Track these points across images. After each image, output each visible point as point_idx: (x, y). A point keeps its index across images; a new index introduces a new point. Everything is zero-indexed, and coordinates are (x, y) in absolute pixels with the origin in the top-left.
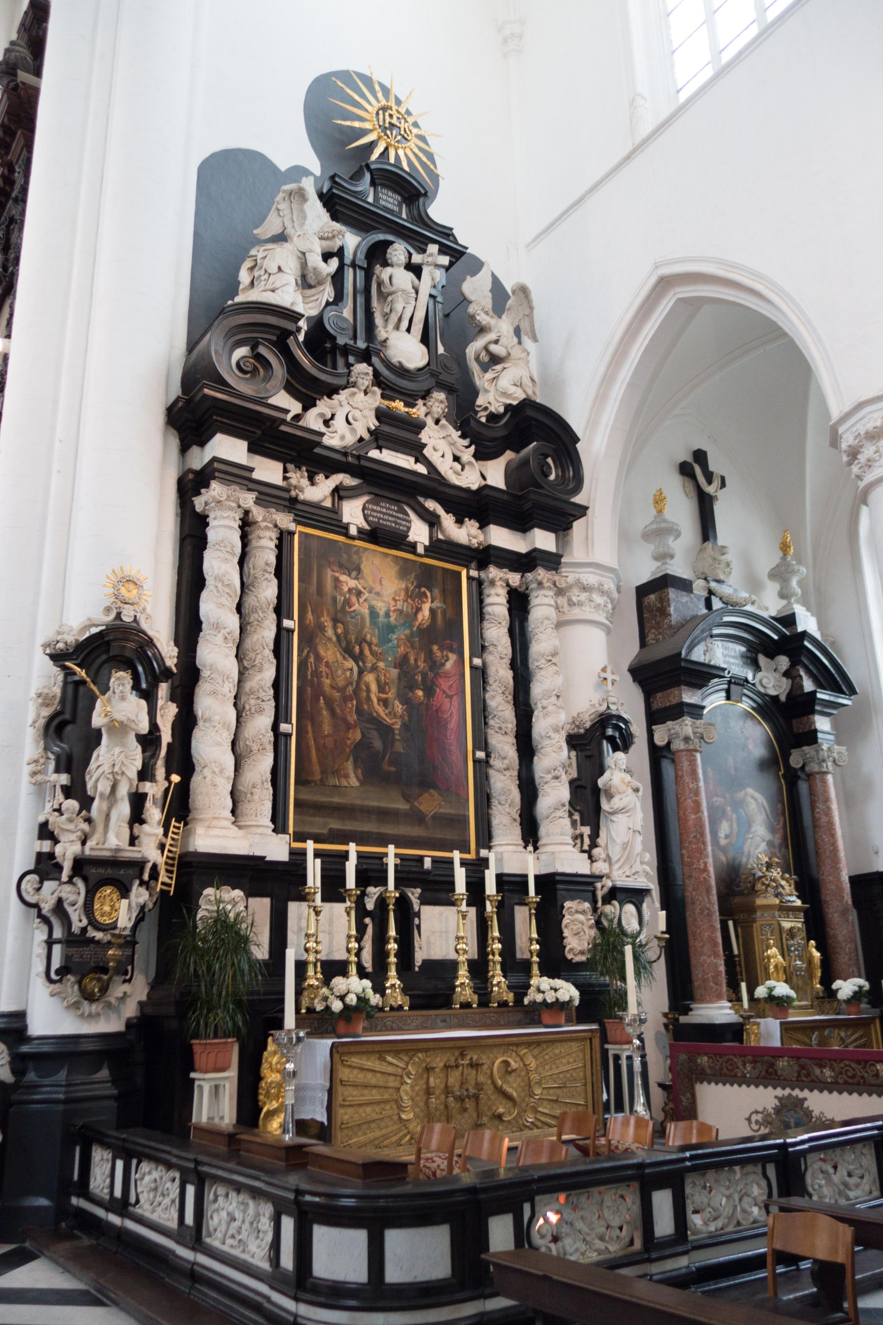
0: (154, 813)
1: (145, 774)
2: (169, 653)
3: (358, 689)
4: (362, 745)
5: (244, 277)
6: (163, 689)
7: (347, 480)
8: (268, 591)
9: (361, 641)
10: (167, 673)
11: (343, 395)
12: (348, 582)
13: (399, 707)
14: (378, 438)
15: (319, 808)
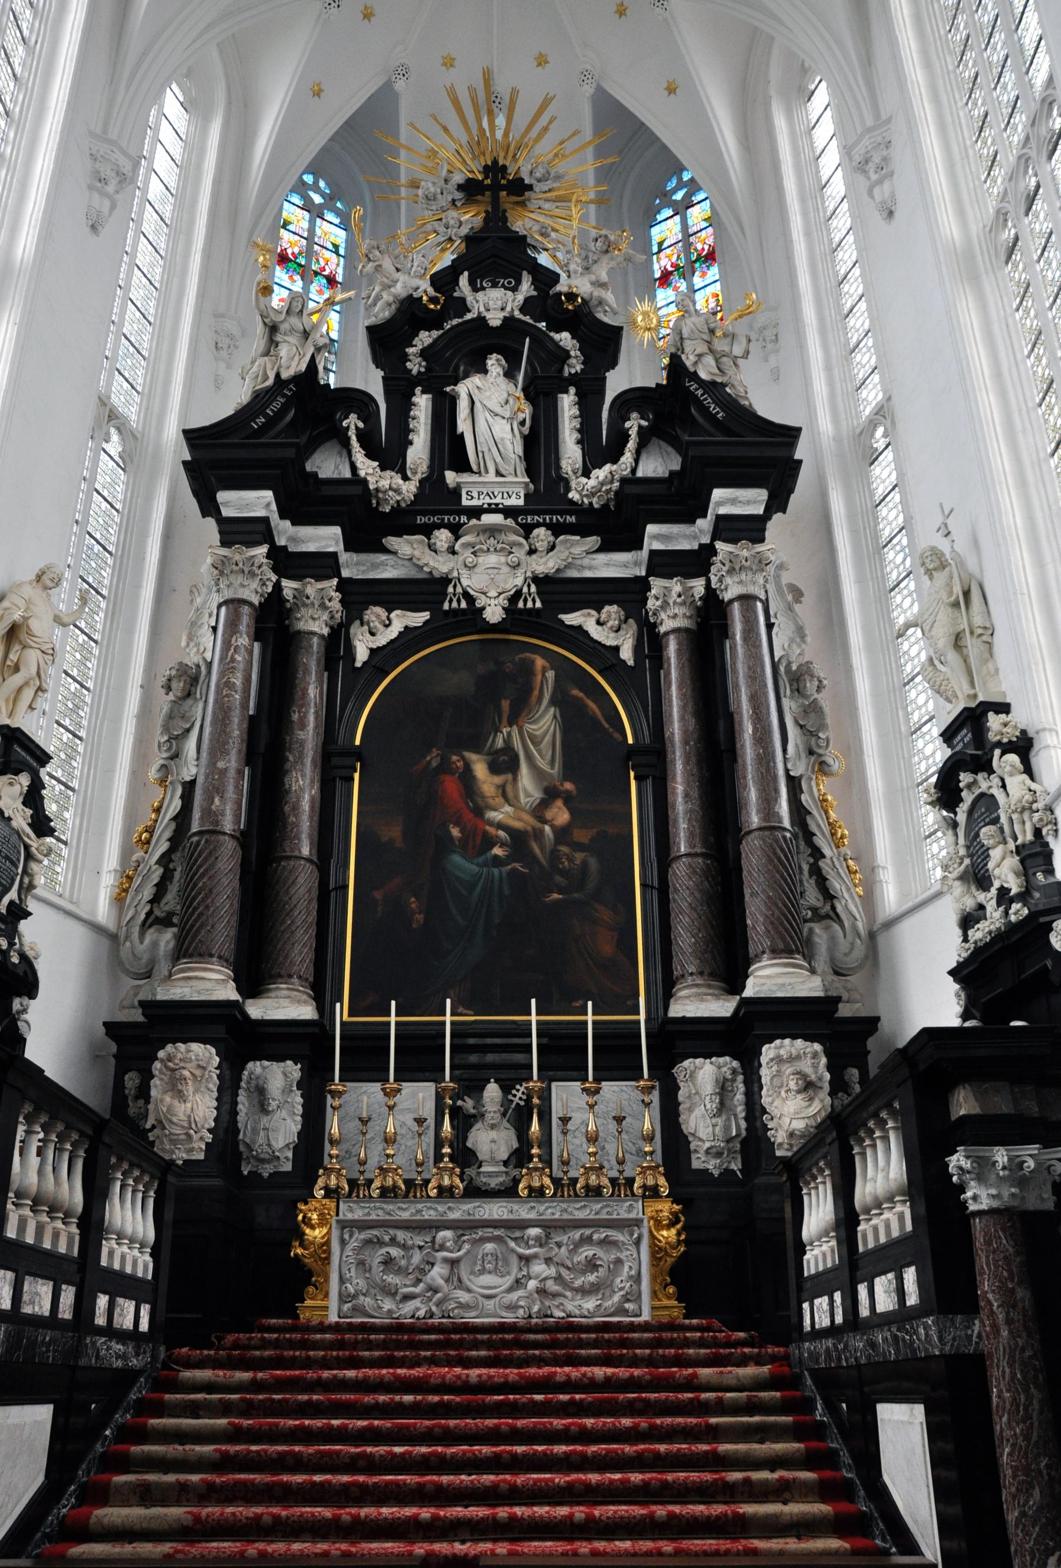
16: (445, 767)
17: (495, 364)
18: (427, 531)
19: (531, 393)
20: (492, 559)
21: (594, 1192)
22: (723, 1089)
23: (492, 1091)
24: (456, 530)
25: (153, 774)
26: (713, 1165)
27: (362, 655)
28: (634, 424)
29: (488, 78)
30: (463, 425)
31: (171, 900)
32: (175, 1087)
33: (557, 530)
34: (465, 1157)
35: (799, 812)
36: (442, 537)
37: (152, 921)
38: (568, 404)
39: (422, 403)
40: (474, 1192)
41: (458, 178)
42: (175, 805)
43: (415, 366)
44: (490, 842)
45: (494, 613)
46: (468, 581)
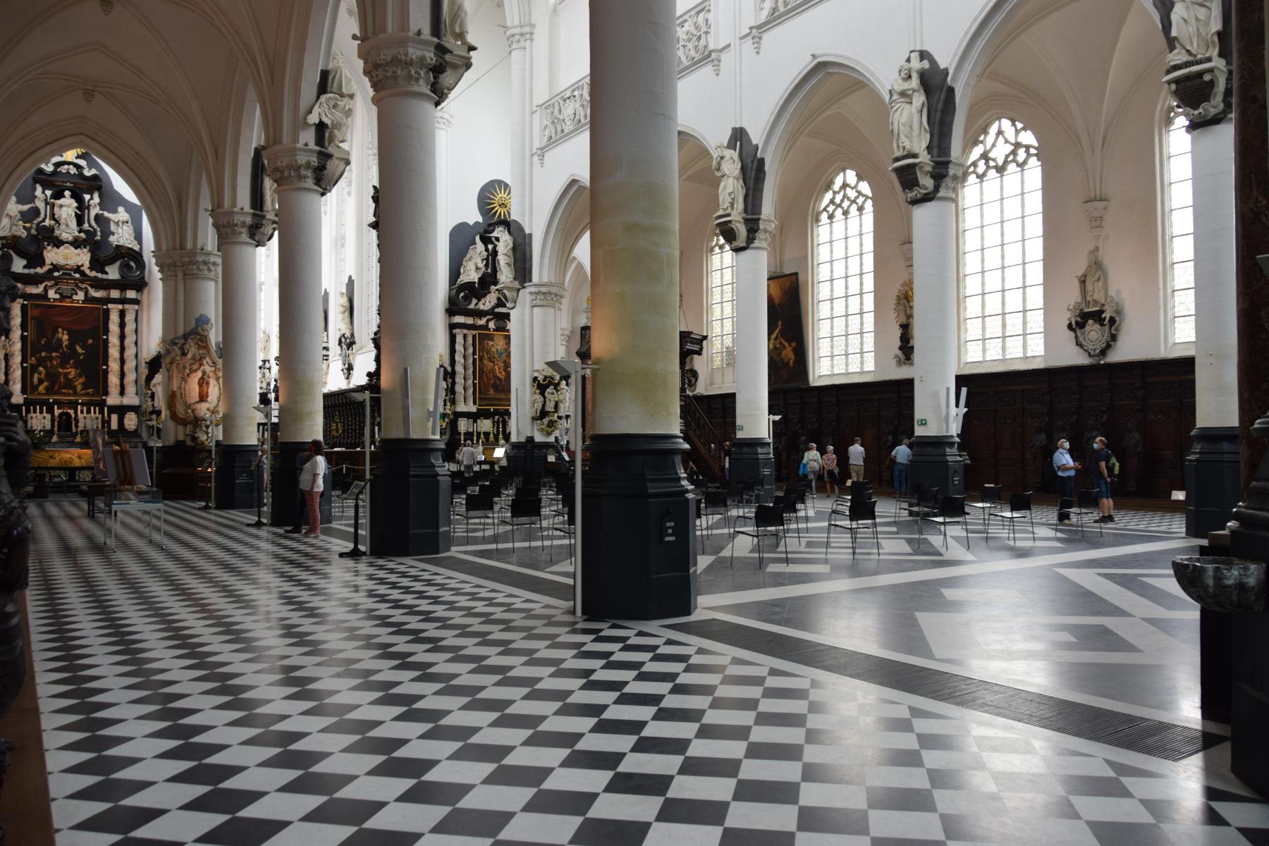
0: (448, 404)
1: (447, 395)
2: (449, 369)
3: (493, 370)
4: (495, 383)
5: (462, 270)
6: (448, 376)
7: (490, 317)
8: (471, 350)
9: (494, 358)
10: (449, 373)
11: (488, 296)
12: (491, 343)
13: (504, 373)
14: (497, 306)
15: (484, 399)
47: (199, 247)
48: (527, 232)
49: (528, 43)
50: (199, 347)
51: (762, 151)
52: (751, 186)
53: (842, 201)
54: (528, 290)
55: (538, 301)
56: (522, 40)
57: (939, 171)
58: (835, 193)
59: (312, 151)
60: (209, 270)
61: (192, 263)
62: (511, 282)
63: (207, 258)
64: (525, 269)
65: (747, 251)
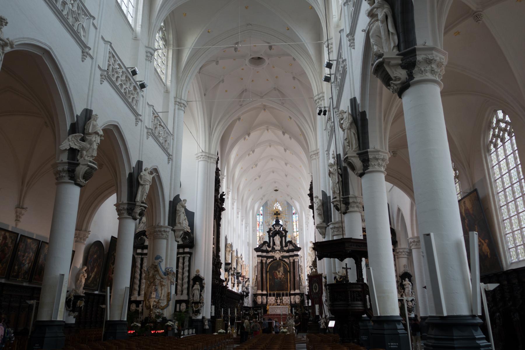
16: (275, 272)
17: (277, 235)
18: (272, 252)
19: (281, 237)
20: (278, 255)
21: (285, 305)
22: (294, 298)
23: (279, 298)
24: (275, 252)
25: (253, 274)
26: (293, 303)
27: (268, 263)
28: (288, 244)
29: (276, 199)
30: (275, 241)
31: (256, 284)
32: (259, 298)
33: (283, 252)
34: (277, 302)
35: (300, 278)
36: (274, 253)
37: (255, 286)
38: (284, 238)
39: (272, 238)
40: (278, 305)
41: (274, 213)
42: (256, 277)
43: (271, 234)
44: (278, 278)
45: (278, 259)
46: (276, 256)
47: (157, 224)
48: (328, 195)
49: (322, 101)
50: (155, 271)
51: (362, 107)
52: (360, 132)
53: (499, 132)
54: (331, 226)
55: (335, 232)
56: (320, 101)
57: (408, 60)
58: (494, 129)
59: (65, 163)
60: (162, 234)
61: (155, 232)
62: (321, 223)
63: (160, 229)
64: (328, 216)
65: (365, 176)
